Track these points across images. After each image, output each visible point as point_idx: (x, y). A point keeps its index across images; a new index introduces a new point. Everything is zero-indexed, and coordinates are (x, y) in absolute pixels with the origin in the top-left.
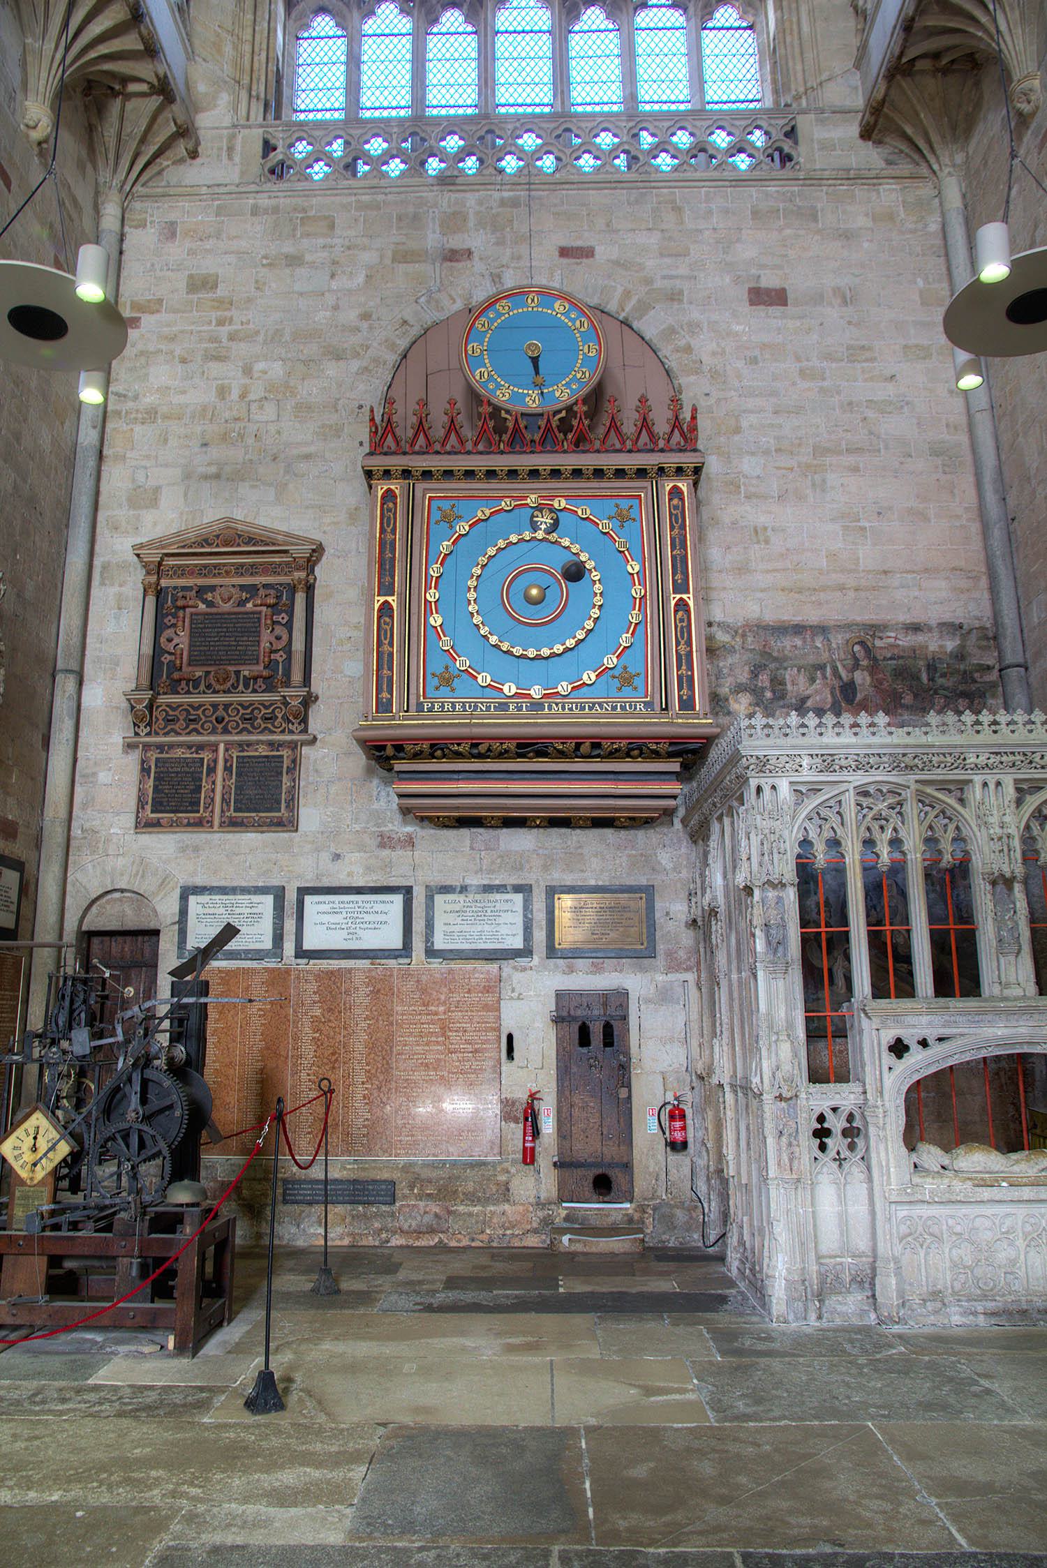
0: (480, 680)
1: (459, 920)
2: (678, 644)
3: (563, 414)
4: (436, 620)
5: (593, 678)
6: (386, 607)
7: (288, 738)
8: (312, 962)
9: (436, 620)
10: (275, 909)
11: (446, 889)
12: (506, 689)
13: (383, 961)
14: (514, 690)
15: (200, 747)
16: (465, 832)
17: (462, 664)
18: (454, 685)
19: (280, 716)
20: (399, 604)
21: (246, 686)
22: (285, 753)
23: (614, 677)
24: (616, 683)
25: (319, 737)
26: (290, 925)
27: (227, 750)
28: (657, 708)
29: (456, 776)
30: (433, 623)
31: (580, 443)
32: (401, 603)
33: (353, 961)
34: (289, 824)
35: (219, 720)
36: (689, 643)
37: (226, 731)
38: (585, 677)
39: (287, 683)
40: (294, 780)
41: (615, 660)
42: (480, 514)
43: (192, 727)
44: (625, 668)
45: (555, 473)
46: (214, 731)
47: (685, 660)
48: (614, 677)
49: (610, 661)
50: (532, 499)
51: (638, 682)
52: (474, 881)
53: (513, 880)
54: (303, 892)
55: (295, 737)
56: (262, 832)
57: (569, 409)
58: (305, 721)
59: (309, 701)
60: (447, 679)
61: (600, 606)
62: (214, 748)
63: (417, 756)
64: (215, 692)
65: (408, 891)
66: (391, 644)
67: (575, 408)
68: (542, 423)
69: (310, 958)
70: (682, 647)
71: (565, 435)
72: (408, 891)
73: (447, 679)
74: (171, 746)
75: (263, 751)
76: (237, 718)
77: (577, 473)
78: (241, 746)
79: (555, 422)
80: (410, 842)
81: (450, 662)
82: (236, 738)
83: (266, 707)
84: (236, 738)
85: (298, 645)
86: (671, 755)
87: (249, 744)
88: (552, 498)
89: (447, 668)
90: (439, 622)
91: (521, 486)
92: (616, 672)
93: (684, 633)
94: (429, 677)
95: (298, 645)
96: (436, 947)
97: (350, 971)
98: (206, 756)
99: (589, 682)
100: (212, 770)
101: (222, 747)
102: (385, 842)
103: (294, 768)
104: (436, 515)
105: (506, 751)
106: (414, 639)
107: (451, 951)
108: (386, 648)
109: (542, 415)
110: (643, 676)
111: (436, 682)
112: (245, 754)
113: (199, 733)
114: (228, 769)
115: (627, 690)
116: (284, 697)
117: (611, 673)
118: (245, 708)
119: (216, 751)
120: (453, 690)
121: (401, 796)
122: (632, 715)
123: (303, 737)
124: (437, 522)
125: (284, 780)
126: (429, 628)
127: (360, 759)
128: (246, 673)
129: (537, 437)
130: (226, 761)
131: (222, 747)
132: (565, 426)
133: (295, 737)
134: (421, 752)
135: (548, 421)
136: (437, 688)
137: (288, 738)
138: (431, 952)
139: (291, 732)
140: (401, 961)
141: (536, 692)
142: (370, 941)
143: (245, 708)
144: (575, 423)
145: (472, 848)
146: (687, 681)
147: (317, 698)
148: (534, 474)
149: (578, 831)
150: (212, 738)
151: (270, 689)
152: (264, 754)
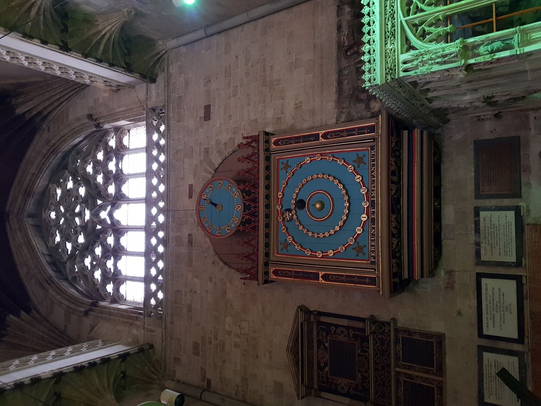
0: (360, 232)
1: (497, 247)
2: (343, 136)
3: (244, 194)
4: (331, 253)
5: (359, 176)
6: (325, 277)
7: (392, 333)
8: (526, 334)
9: (331, 253)
10: (492, 352)
11: (478, 254)
12: (364, 219)
13: (525, 292)
14: (364, 215)
15: (398, 381)
16: (446, 243)
17: (352, 241)
18: (362, 245)
19: (381, 336)
20: (322, 270)
21: (366, 352)
22: (400, 336)
23: (359, 167)
24: (361, 165)
25: (392, 317)
26: (503, 345)
27: (399, 367)
28: (372, 144)
29: (411, 246)
30: (332, 255)
31: (256, 186)
32: (322, 269)
33: (525, 310)
34: (440, 338)
35: (383, 369)
36: (342, 131)
37: (389, 366)
38: (358, 180)
39: (364, 330)
40: (415, 332)
41: (350, 166)
42: (284, 231)
43: (387, 384)
44: (354, 161)
45: (267, 197)
46: (390, 372)
47: (350, 132)
48: (359, 167)
49: (350, 169)
50: (279, 208)
51: (361, 155)
52: (472, 238)
53: (472, 217)
54: (481, 334)
55: (392, 329)
56: (445, 353)
57: (243, 191)
58: (383, 323)
59: (373, 320)
60: (359, 249)
61: (323, 174)
62: (398, 374)
63: (400, 265)
64: (369, 368)
65: (479, 276)
66: (342, 276)
67: (242, 189)
68: (247, 203)
69: (524, 334)
70: (344, 134)
71: (252, 193)
72: (479, 276)
73: (359, 249)
74: (397, 397)
75: (400, 347)
76: (383, 359)
77: (267, 187)
78: (397, 359)
79: (247, 198)
80: (450, 273)
81: (351, 247)
82: (392, 361)
83: (377, 343)
84: (392, 361)
85: (345, 322)
86: (399, 136)
87: (396, 354)
88: (278, 198)
89: (354, 249)
90: (332, 252)
91: (273, 211)
92: (356, 165)
93: (337, 134)
94: (358, 258)
95: (345, 322)
96: (515, 261)
97: (531, 313)
98: (402, 379)
99: (361, 178)
100: (410, 376)
101: (397, 369)
102: (450, 286)
103: (409, 331)
104: (284, 251)
105: (396, 219)
106: (339, 264)
107: (517, 253)
108: (344, 278)
109: (244, 203)
110: (358, 153)
111: (361, 255)
112: (401, 357)
113: (390, 380)
114: (409, 368)
115: (365, 160)
116: (371, 333)
117: (356, 168)
118: (377, 354)
119: (400, 373)
120: (365, 246)
121: (422, 276)
122: (377, 156)
123: (392, 325)
124: (288, 251)
125: (415, 338)
126: (334, 257)
127: (405, 296)
128: (359, 351)
129: (253, 205)
130: (405, 368)
131: (397, 369)
132: (249, 193)
133: (392, 329)
134: (397, 263)
135: (246, 200)
136: (364, 254)
137: (392, 333)
138: (518, 264)
139: (389, 331)
140: (524, 281)
141: (366, 205)
142: (512, 298)
143: (377, 354)
144: (247, 189)
145: (453, 239)
146: (361, 130)
147: (372, 316)
148: (267, 206)
149: (443, 183)
150: (393, 374)
151: (367, 339)
152: (401, 347)
